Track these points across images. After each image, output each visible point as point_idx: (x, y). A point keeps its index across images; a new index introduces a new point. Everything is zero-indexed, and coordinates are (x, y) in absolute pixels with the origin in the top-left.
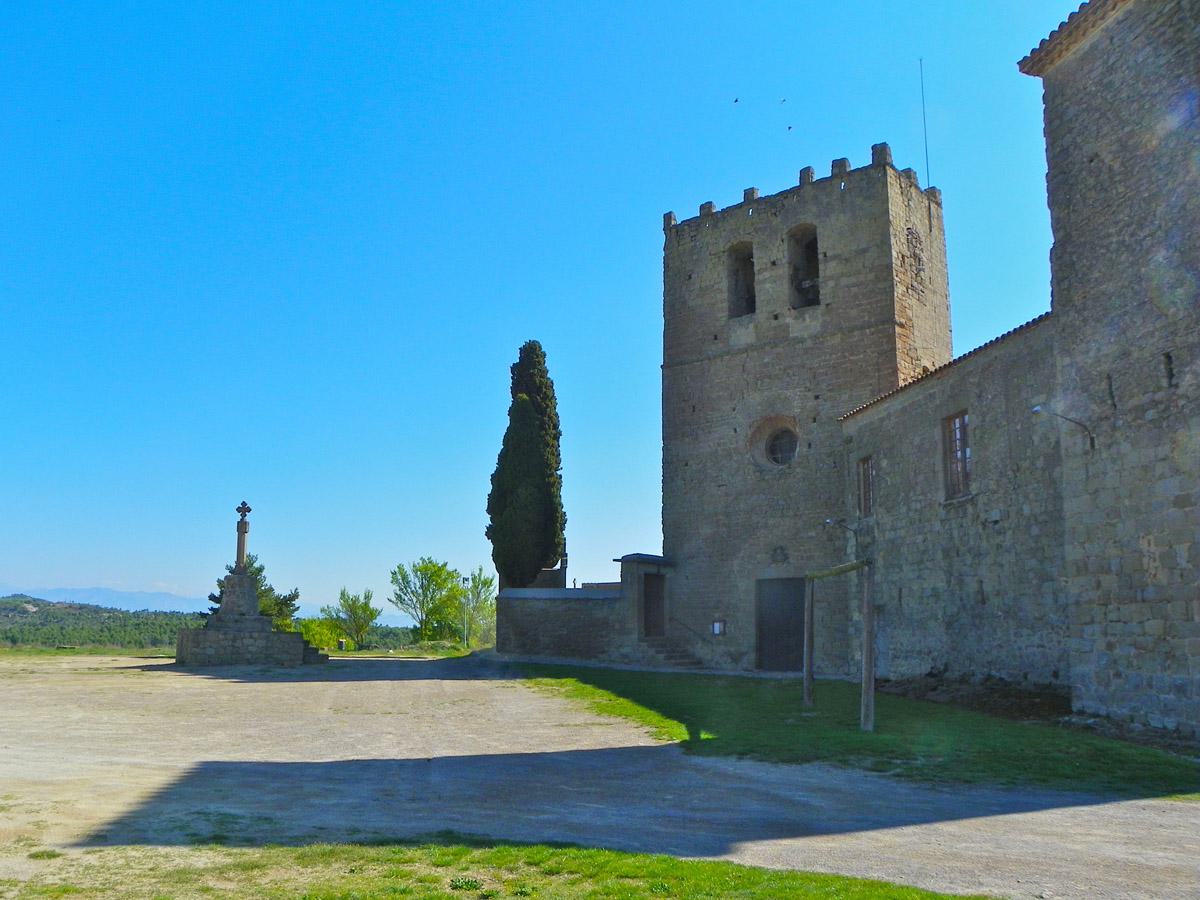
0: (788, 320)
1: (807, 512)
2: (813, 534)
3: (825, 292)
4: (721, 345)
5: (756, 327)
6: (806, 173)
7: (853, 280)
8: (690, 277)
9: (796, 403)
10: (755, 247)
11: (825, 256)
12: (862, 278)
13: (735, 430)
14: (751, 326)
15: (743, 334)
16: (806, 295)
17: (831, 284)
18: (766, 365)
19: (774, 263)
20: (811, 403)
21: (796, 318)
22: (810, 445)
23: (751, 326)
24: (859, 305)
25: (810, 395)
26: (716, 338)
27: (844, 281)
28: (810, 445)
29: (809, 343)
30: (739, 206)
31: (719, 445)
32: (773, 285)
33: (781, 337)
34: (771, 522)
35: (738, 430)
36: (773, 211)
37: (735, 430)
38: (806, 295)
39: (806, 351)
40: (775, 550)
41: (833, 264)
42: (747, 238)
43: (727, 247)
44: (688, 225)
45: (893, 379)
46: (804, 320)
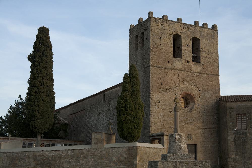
0: (191, 65)
1: (197, 124)
2: (199, 131)
3: (202, 60)
4: (171, 65)
5: (182, 63)
6: (196, 23)
7: (209, 60)
8: (160, 38)
9: (194, 92)
10: (182, 38)
11: (202, 49)
12: (211, 60)
13: (176, 95)
14: (181, 62)
15: (178, 64)
16: (196, 59)
17: (204, 58)
18: (185, 76)
19: (188, 45)
20: (199, 92)
21: (194, 65)
22: (198, 104)
23: (181, 62)
24: (210, 68)
25: (198, 89)
26: (169, 62)
27: (207, 59)
28: (198, 104)
29: (198, 74)
30: (177, 22)
31: (170, 98)
32: (187, 51)
33: (189, 70)
34: (187, 126)
35: (177, 95)
36: (188, 29)
37: (176, 95)
38: (196, 59)
39: (197, 76)
40: (189, 135)
41: (204, 53)
42: (180, 34)
43: (174, 34)
44: (160, 20)
45: (219, 91)
46: (196, 66)
